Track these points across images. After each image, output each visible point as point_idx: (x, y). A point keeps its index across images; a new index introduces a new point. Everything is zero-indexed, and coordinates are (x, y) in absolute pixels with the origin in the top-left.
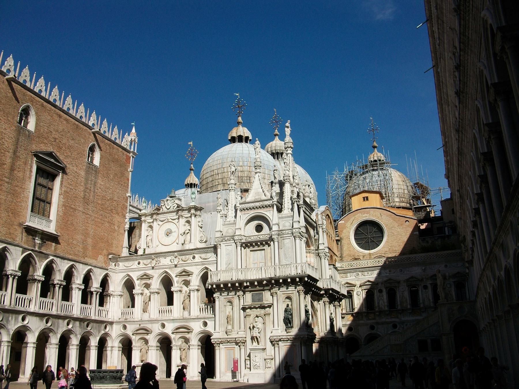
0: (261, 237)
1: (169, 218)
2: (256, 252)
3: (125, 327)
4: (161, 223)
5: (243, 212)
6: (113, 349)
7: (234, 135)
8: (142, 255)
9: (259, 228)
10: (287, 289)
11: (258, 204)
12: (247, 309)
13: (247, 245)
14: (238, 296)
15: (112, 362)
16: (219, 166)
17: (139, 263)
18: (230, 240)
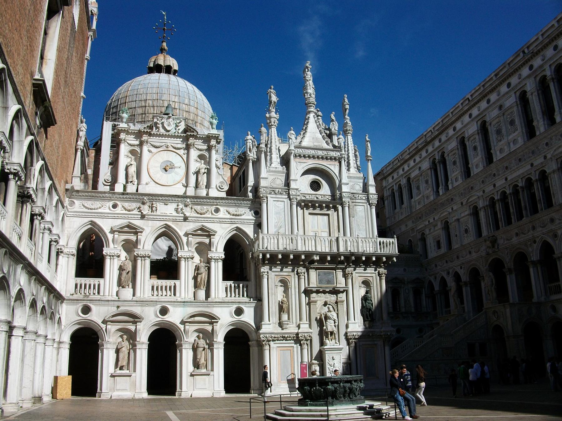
0: (320, 197)
1: (169, 144)
2: (316, 216)
3: (86, 310)
4: (154, 150)
5: (298, 159)
6: (62, 345)
7: (161, 62)
8: (132, 194)
9: (315, 186)
10: (365, 270)
11: (320, 153)
12: (312, 292)
13: (306, 204)
14: (298, 273)
15: (58, 368)
16: (155, 97)
17: (115, 206)
18: (281, 194)
